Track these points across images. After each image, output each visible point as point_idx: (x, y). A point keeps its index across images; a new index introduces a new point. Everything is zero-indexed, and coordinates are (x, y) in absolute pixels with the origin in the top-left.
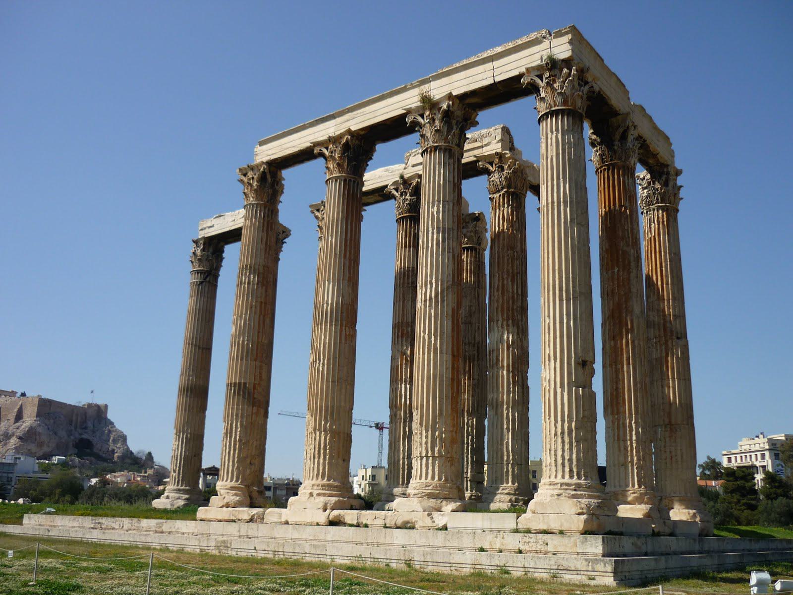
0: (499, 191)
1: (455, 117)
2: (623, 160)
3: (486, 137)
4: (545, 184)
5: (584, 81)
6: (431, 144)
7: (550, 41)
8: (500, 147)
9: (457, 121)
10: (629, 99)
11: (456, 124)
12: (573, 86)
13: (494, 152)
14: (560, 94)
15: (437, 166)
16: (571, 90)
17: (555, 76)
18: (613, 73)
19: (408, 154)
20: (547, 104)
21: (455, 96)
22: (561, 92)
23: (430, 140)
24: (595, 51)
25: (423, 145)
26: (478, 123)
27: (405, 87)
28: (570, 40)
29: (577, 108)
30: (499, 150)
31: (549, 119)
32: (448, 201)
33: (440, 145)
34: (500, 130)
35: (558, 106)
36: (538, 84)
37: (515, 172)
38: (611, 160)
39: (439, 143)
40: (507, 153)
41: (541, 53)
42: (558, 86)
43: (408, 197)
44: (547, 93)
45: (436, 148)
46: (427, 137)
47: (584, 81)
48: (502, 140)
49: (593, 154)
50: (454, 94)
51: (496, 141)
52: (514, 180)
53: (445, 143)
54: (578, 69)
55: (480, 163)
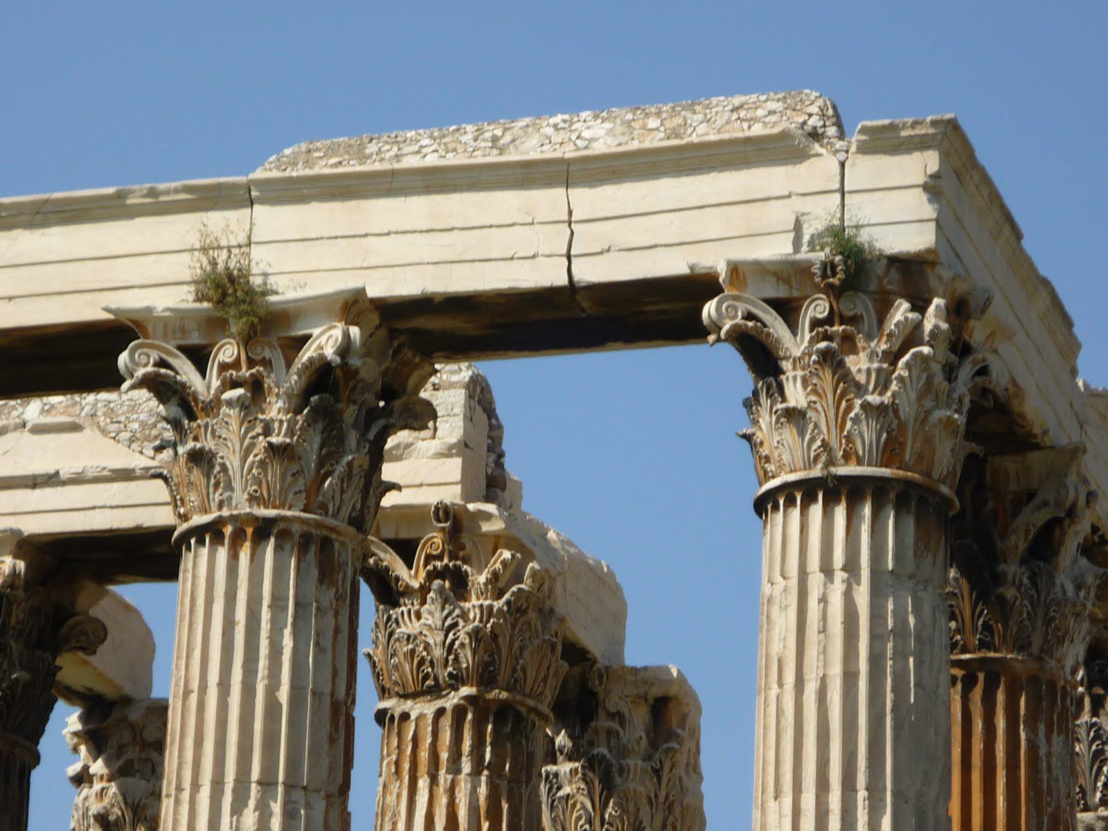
0: (436, 691)
2: (1035, 649)
4: (787, 801)
6: (244, 508)
7: (842, 156)
8: (457, 476)
10: (1074, 372)
12: (930, 379)
15: (265, 615)
16: (919, 399)
17: (853, 320)
18: (1046, 283)
20: (812, 440)
21: (372, 301)
23: (237, 485)
25: (193, 498)
27: (120, 195)
28: (932, 176)
29: (935, 475)
32: (305, 788)
35: (860, 462)
36: (778, 341)
37: (519, 610)
38: (984, 645)
39: (282, 506)
40: (488, 516)
42: (869, 371)
44: (815, 392)
45: (263, 529)
46: (224, 468)
48: (463, 447)
50: (375, 291)
53: (305, 510)
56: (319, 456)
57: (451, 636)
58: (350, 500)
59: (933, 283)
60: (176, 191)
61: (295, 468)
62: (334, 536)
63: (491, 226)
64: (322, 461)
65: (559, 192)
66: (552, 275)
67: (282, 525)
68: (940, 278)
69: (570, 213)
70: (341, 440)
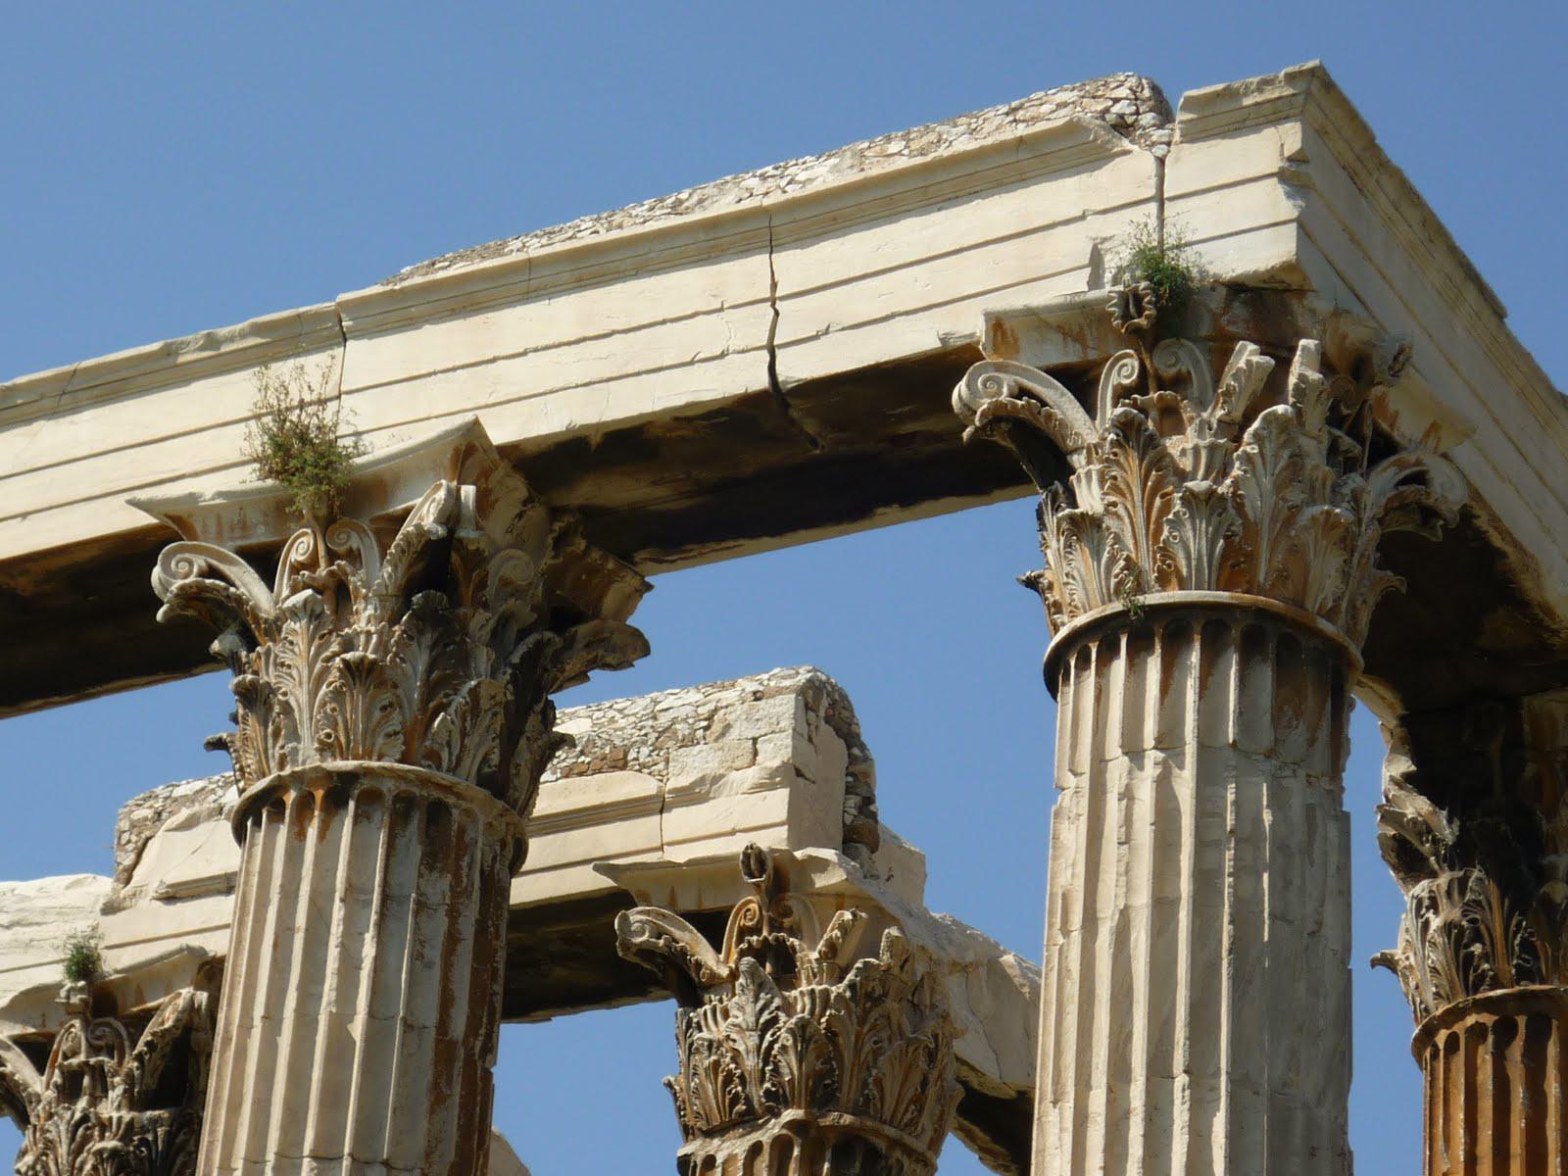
0: (748, 1120)
1: (489, 593)
3: (689, 741)
4: (1069, 1104)
5: (1368, 432)
6: (308, 757)
7: (1160, 151)
8: (782, 814)
9: (504, 621)
11: (496, 638)
12: (1296, 461)
13: (736, 846)
14: (1204, 504)
15: (338, 912)
16: (1278, 488)
17: (1179, 382)
19: (145, 812)
20: (1113, 560)
21: (508, 451)
22: (1211, 494)
23: (305, 732)
24: (1453, 250)
25: (250, 761)
26: (645, 650)
27: (169, 352)
28: (1290, 159)
29: (1312, 605)
30: (774, 840)
31: (1119, 666)
32: (386, 1164)
33: (368, 772)
34: (784, 708)
36: (1063, 424)
37: (869, 996)
38: (1524, 974)
39: (368, 755)
40: (822, 865)
41: (1097, 227)
42: (1196, 450)
43: (111, 1108)
45: (339, 790)
46: (287, 709)
47: (1368, 432)
48: (793, 774)
49: (1407, 921)
50: (501, 431)
51: (752, 775)
52: (858, 1050)
54: (1332, 351)
55: (635, 916)
56: (427, 681)
57: (768, 1038)
58: (479, 746)
59: (1303, 320)
60: (243, 335)
61: (386, 697)
62: (451, 800)
63: (664, 322)
64: (431, 689)
65: (759, 262)
66: (748, 377)
67: (366, 784)
68: (1313, 312)
69: (774, 286)
70: (463, 663)
